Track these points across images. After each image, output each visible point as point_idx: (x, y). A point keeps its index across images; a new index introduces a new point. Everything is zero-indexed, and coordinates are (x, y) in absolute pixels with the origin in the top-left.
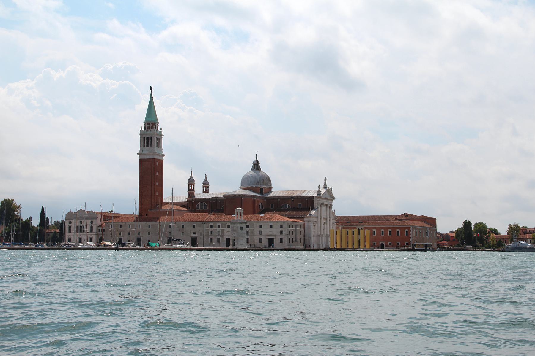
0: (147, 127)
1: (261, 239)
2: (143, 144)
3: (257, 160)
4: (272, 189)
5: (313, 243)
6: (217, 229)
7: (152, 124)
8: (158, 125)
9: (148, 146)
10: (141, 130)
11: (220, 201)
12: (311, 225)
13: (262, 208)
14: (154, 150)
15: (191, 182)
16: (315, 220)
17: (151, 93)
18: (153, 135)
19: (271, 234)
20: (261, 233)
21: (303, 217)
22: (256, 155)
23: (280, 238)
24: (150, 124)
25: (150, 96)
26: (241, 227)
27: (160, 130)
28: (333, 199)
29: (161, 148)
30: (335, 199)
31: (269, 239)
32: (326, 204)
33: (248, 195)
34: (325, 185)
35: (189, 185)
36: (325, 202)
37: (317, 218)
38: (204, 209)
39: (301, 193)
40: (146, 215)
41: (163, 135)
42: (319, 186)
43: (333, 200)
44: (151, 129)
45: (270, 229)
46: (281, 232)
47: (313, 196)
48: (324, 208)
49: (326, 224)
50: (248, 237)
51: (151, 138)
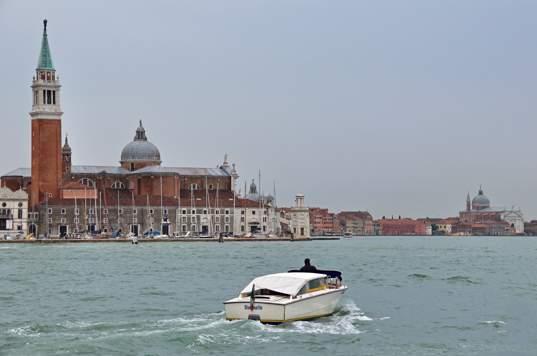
0: (47, 76)
9: (49, 103)
24: (51, 73)
31: (251, 227)
40: (50, 195)
45: (252, 216)
50: (228, 225)
51: (54, 92)
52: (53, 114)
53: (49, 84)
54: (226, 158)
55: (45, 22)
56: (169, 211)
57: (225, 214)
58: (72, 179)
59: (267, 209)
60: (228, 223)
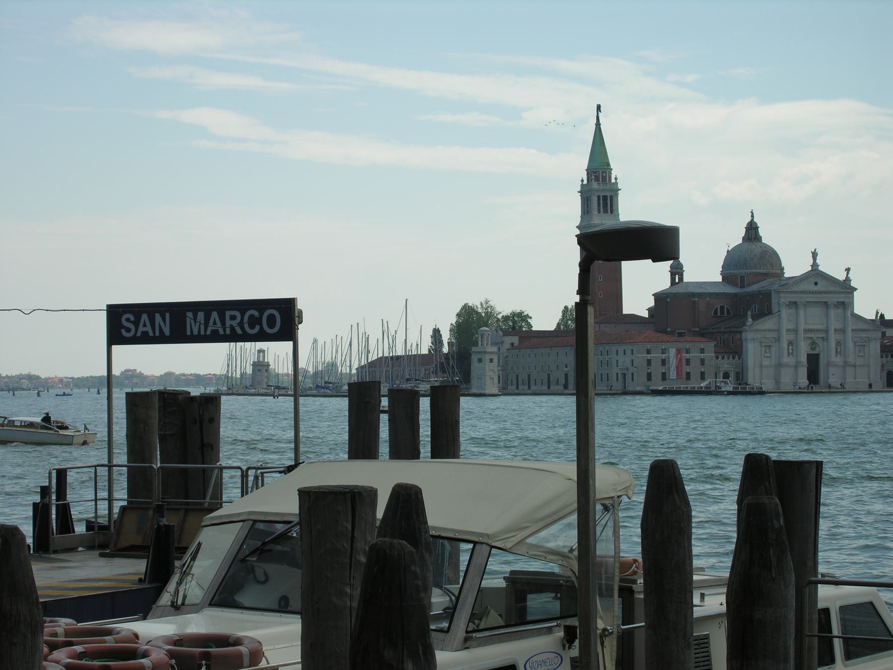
1: (617, 374)
10: (582, 185)
13: (726, 315)
21: (741, 332)
22: (752, 212)
24: (590, 173)
25: (595, 122)
26: (479, 359)
29: (615, 213)
30: (857, 289)
33: (678, 293)
37: (779, 331)
41: (620, 190)
47: (771, 290)
48: (816, 311)
49: (827, 340)
50: (609, 372)
55: (599, 107)
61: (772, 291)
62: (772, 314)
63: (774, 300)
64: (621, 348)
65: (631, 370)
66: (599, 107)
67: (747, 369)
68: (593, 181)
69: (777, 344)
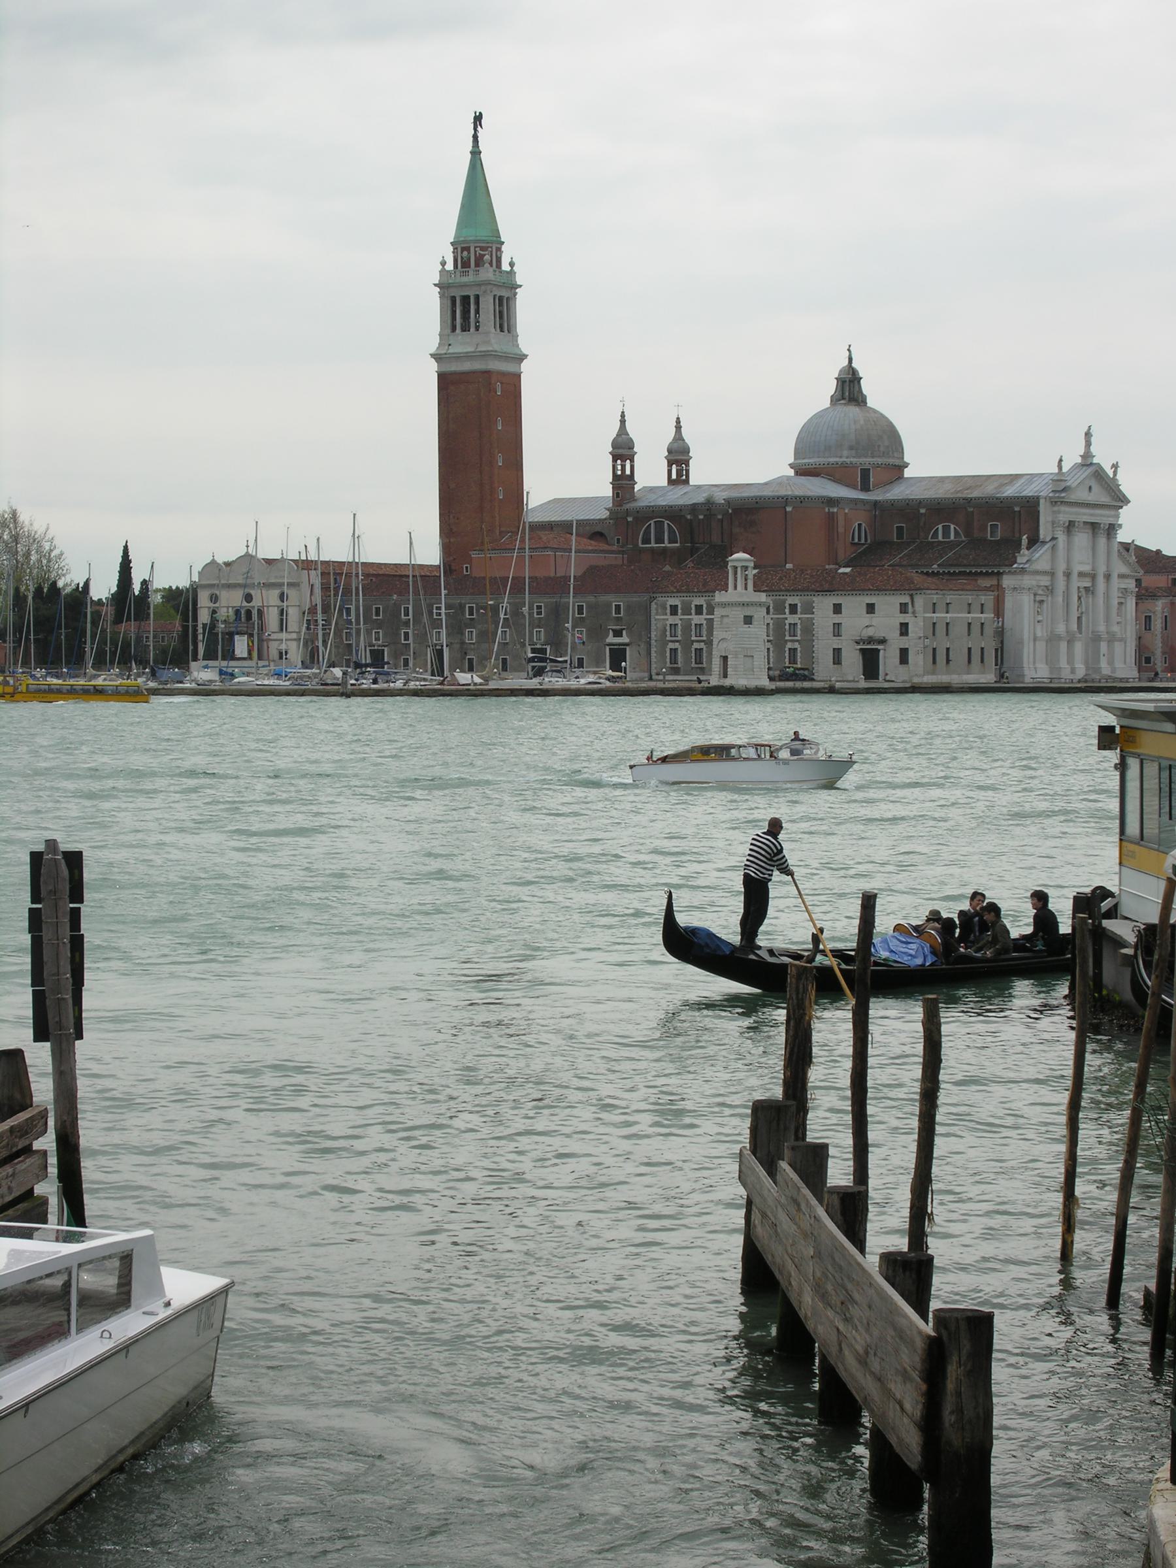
0: (462, 257)
1: (837, 653)
2: (449, 322)
3: (854, 365)
4: (906, 470)
5: (1034, 663)
6: (692, 619)
7: (478, 249)
8: (502, 252)
9: (465, 328)
10: (443, 272)
11: (720, 517)
12: (1026, 600)
13: (863, 541)
14: (488, 342)
15: (623, 450)
16: (1045, 581)
17: (475, 138)
18: (483, 287)
19: (871, 634)
20: (837, 629)
21: (999, 574)
22: (849, 350)
23: (901, 649)
24: (472, 250)
27: (508, 269)
28: (1121, 504)
30: (1129, 502)
31: (863, 651)
32: (1092, 524)
34: (1087, 455)
35: (615, 460)
36: (1086, 515)
37: (1052, 574)
38: (666, 544)
39: (1002, 485)
42: (1061, 460)
43: (1121, 507)
44: (477, 265)
45: (866, 619)
46: (904, 629)
47: (1038, 498)
48: (1082, 539)
50: (797, 645)
51: (477, 297)
52: (468, 357)
53: (465, 279)
54: (1088, 444)
55: (478, 119)
56: (629, 608)
57: (787, 615)
58: (628, 522)
59: (912, 596)
60: (797, 641)
61: (1042, 501)
62: (1044, 543)
63: (1045, 516)
64: (853, 605)
65: (896, 642)
66: (478, 119)
67: (1021, 642)
68: (487, 265)
69: (1050, 598)
